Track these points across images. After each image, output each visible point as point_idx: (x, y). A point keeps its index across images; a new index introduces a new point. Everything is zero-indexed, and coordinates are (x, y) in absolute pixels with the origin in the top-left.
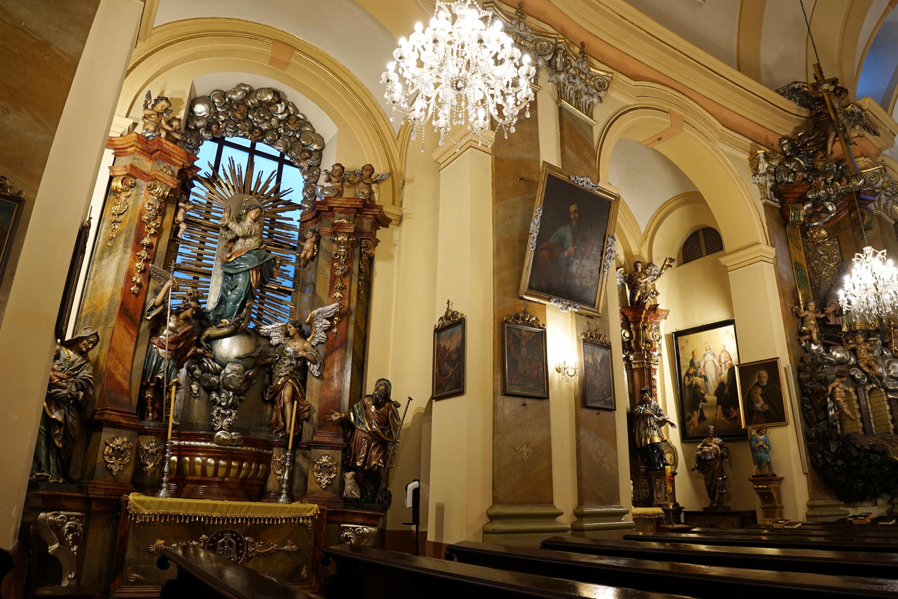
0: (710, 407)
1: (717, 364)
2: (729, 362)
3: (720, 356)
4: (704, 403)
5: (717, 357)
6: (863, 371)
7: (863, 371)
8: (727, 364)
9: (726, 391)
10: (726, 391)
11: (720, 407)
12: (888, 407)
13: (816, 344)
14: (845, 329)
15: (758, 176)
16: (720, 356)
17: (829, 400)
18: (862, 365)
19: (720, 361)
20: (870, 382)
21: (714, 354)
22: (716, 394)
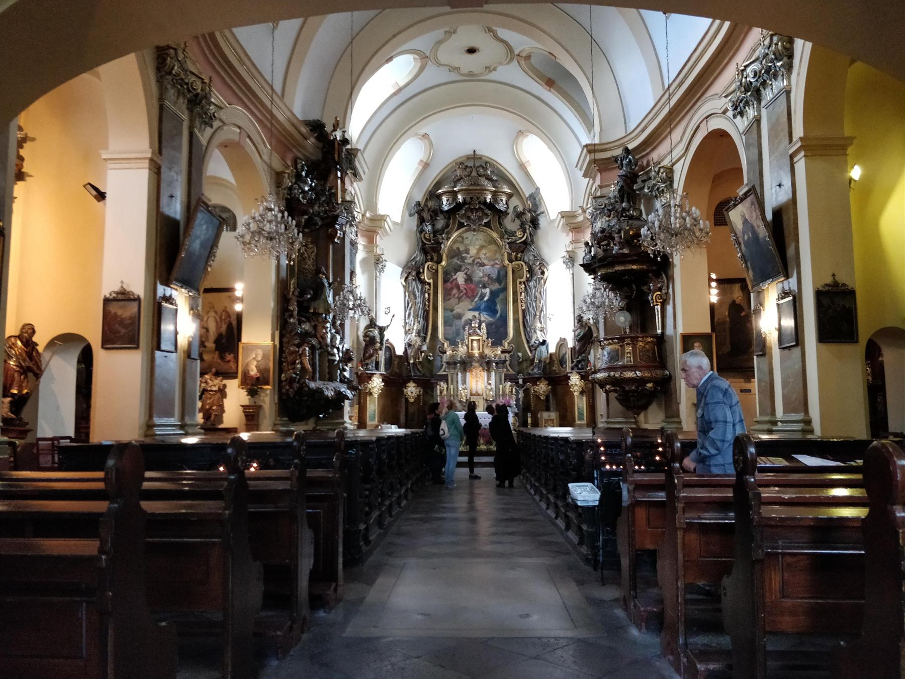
0: (210, 352)
1: (218, 320)
2: (228, 319)
3: (221, 314)
4: (204, 349)
5: (219, 314)
6: (319, 341)
7: (319, 341)
8: (227, 321)
9: (224, 341)
10: (224, 341)
11: (217, 352)
12: (327, 364)
13: (294, 318)
14: (312, 311)
15: (280, 189)
16: (221, 314)
17: (298, 357)
18: (318, 336)
19: (221, 318)
20: (321, 348)
21: (216, 312)
22: (216, 342)
